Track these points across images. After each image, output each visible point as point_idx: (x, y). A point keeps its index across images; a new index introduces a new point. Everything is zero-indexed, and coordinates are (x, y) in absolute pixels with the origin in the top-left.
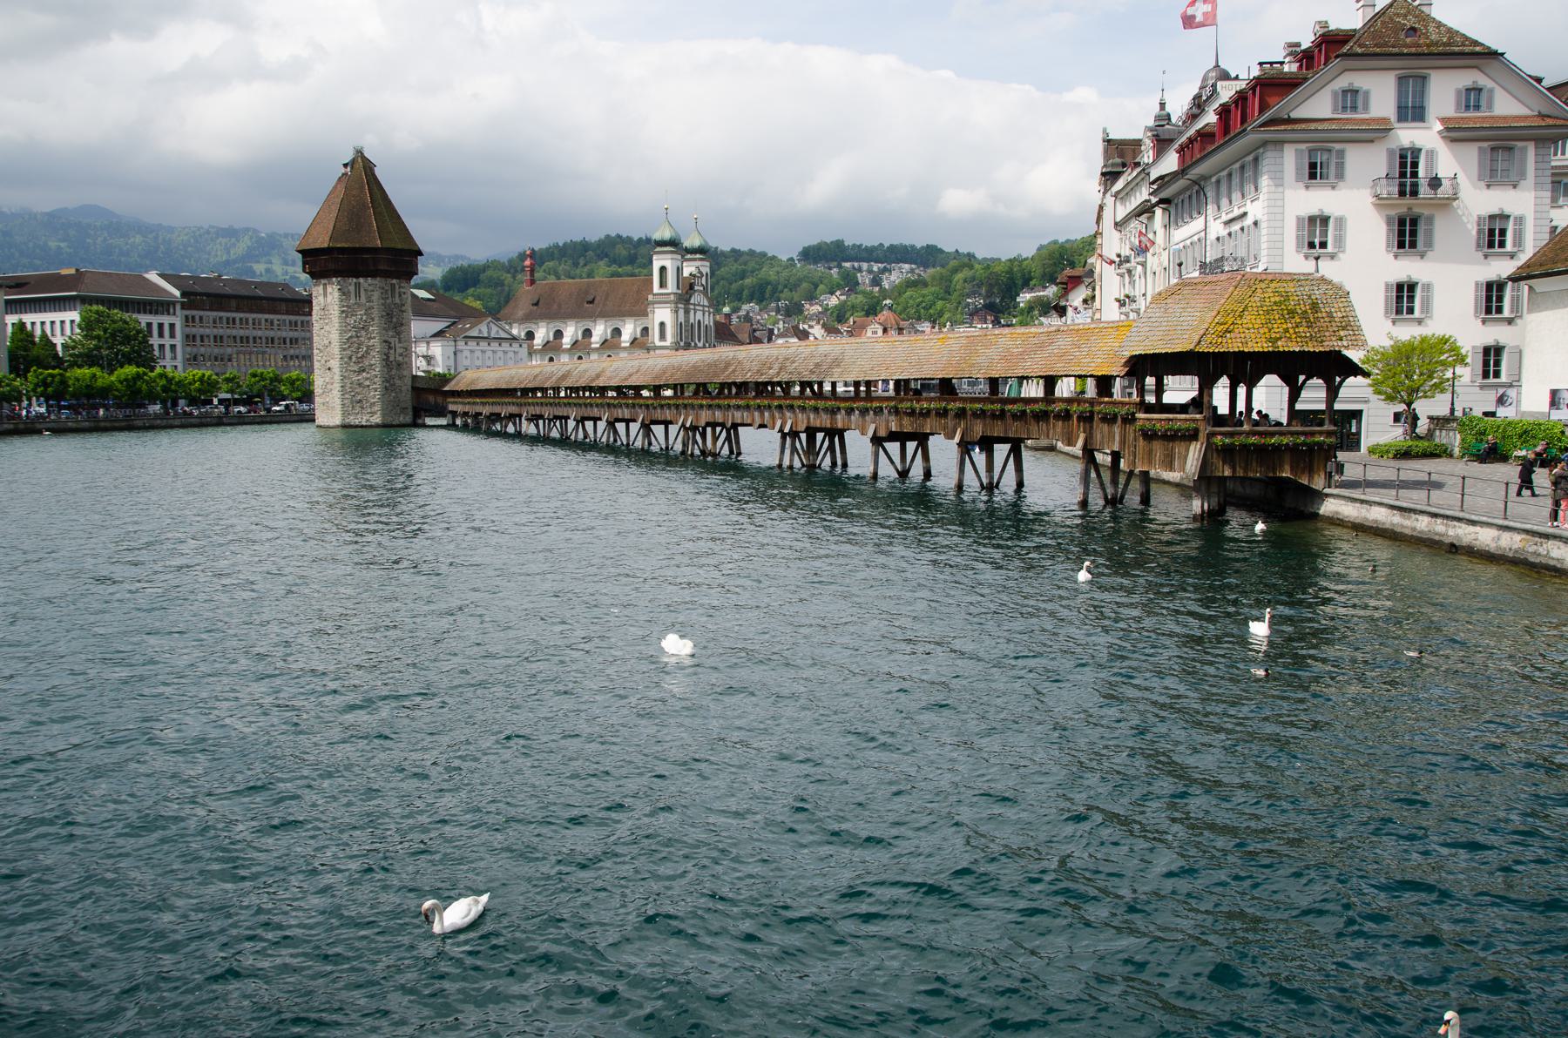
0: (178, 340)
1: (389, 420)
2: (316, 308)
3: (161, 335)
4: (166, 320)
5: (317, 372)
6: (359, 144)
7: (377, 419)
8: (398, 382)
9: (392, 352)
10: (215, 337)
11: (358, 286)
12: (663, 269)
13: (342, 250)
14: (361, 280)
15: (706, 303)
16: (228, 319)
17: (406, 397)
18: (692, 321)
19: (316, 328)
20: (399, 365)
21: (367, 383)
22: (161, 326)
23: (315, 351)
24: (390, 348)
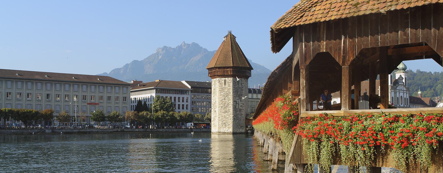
0: (189, 103)
1: (235, 131)
3: (183, 101)
4: (185, 96)
5: (212, 113)
6: (230, 30)
8: (240, 117)
11: (225, 81)
13: (219, 68)
14: (226, 79)
15: (405, 89)
17: (243, 122)
18: (398, 96)
19: (212, 96)
20: (240, 110)
22: (183, 98)
23: (212, 105)
24: (237, 104)
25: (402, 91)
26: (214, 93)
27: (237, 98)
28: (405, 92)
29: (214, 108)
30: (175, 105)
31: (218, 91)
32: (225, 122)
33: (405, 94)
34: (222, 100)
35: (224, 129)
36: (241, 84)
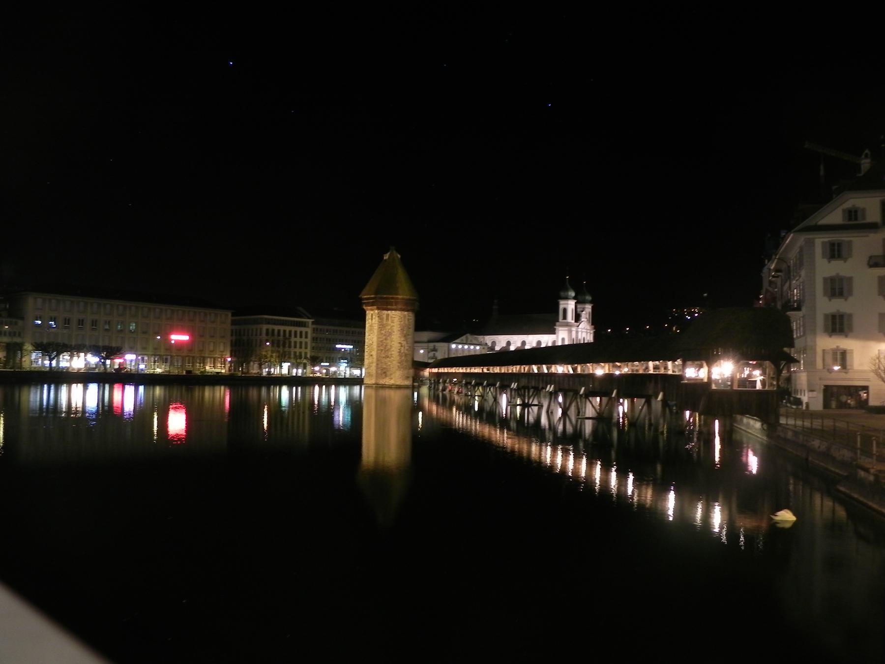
0: (309, 340)
1: (398, 383)
2: (367, 326)
3: (301, 337)
4: (304, 329)
7: (392, 382)
9: (403, 348)
10: (327, 339)
12: (565, 310)
14: (389, 312)
16: (334, 330)
21: (389, 364)
22: (301, 333)
23: (366, 347)
25: (585, 331)
26: (371, 330)
27: (403, 339)
28: (588, 331)
29: (369, 352)
30: (290, 342)
31: (376, 328)
32: (385, 370)
33: (589, 334)
34: (382, 341)
35: (384, 380)
36: (408, 320)
